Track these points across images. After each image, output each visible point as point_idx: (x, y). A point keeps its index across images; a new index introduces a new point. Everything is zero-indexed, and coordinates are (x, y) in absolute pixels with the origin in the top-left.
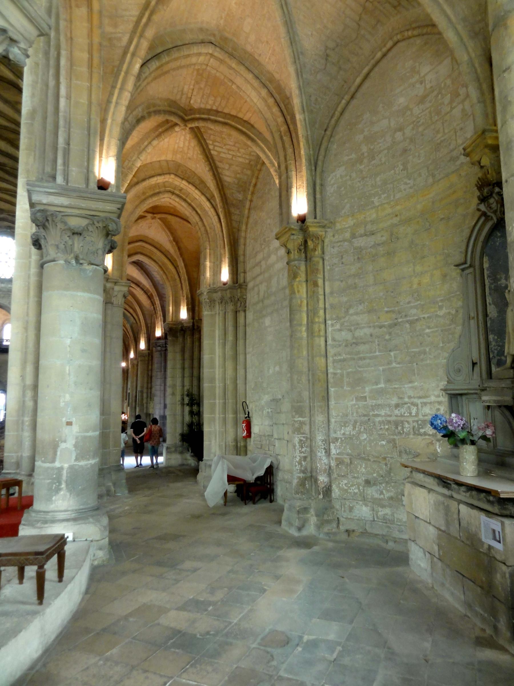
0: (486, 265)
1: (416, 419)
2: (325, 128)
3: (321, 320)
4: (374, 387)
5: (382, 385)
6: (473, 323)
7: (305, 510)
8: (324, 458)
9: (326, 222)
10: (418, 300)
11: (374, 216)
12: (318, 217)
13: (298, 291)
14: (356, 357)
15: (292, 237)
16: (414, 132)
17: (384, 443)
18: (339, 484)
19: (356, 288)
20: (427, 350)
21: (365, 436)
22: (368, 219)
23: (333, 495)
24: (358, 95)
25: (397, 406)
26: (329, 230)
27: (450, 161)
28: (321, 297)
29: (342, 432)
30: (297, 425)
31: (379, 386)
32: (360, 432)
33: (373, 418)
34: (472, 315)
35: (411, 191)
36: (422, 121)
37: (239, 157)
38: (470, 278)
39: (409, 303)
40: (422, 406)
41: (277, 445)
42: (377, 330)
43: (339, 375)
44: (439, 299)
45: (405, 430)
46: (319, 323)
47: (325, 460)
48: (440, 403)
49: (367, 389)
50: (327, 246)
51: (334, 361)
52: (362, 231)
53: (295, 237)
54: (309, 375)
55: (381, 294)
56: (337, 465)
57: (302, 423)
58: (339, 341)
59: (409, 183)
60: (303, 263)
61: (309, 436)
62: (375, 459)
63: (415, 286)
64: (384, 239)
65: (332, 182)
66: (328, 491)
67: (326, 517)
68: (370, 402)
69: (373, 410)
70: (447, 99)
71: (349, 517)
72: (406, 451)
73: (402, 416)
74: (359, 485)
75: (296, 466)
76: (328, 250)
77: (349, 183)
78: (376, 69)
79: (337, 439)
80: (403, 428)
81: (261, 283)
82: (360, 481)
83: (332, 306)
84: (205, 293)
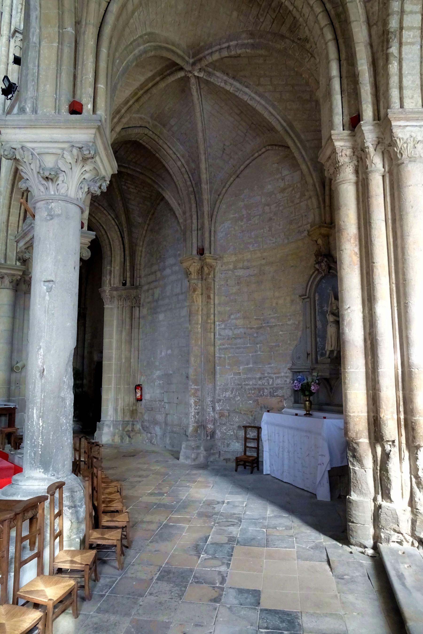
0: (317, 298)
1: (272, 387)
2: (219, 193)
3: (212, 321)
4: (246, 366)
5: (251, 366)
6: (308, 331)
7: (198, 447)
8: (211, 413)
9: (217, 256)
10: (276, 314)
11: (249, 256)
12: (212, 253)
13: (196, 301)
14: (234, 347)
15: (194, 264)
16: (277, 209)
17: (251, 402)
18: (221, 429)
19: (236, 302)
20: (280, 345)
21: (239, 398)
22: (245, 258)
23: (217, 437)
24: (241, 176)
25: (260, 379)
26: (219, 262)
27: (298, 232)
28: (212, 306)
29: (224, 395)
30: (193, 391)
31: (249, 366)
32: (235, 396)
33: (244, 386)
34: (308, 326)
35: (274, 245)
36: (282, 203)
37: (143, 192)
38: (308, 305)
39: (270, 315)
40: (276, 379)
41: (167, 407)
42: (249, 330)
43: (222, 359)
44: (288, 314)
45: (265, 394)
46: (211, 323)
47: (212, 414)
48: (287, 377)
49: (241, 367)
50: (217, 272)
51: (220, 349)
52: (241, 265)
53: (196, 264)
54: (201, 358)
55: (253, 307)
56: (220, 417)
57: (196, 390)
58: (224, 336)
59: (272, 240)
60: (200, 282)
61: (200, 399)
62: (245, 413)
63: (274, 305)
64: (255, 272)
65: (222, 230)
66: (213, 434)
67: (212, 451)
68: (243, 376)
69: (245, 381)
70: (298, 195)
71: (227, 450)
72: (265, 406)
73: (263, 385)
74: (234, 429)
75: (192, 418)
76: (218, 275)
77: (233, 232)
78: (254, 162)
79: (220, 400)
80: (263, 392)
81: (156, 288)
82: (234, 427)
83: (219, 312)
84: (107, 291)
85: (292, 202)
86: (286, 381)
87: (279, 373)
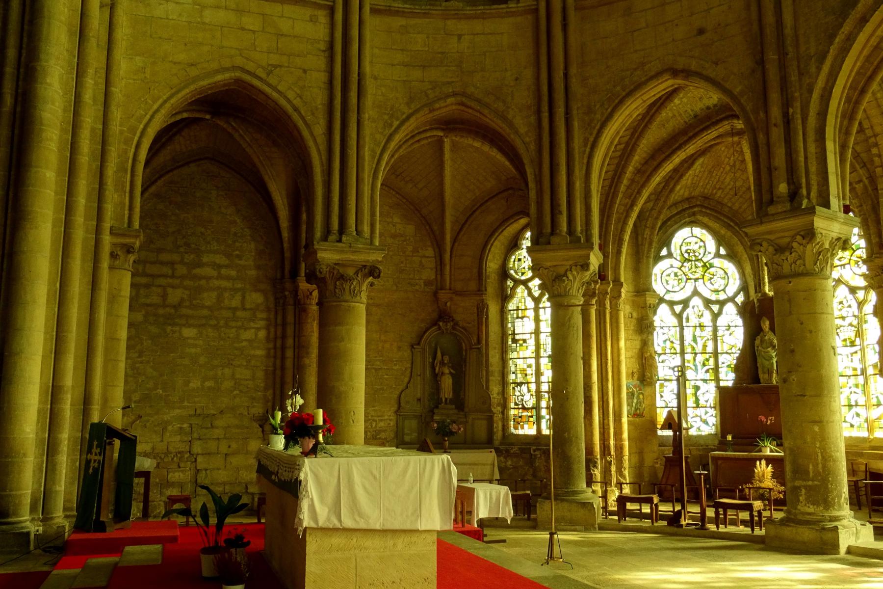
35: (382, 288)
39: (376, 357)
44: (394, 360)
48: (390, 420)
63: (380, 348)
70: (410, 248)
85: (404, 253)
86: (389, 424)
87: (382, 416)
